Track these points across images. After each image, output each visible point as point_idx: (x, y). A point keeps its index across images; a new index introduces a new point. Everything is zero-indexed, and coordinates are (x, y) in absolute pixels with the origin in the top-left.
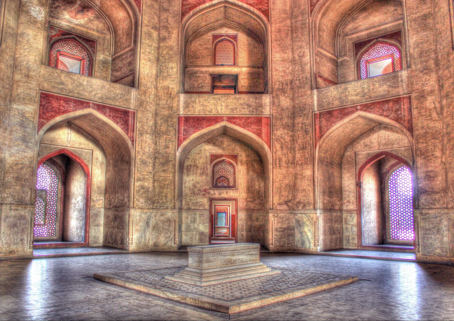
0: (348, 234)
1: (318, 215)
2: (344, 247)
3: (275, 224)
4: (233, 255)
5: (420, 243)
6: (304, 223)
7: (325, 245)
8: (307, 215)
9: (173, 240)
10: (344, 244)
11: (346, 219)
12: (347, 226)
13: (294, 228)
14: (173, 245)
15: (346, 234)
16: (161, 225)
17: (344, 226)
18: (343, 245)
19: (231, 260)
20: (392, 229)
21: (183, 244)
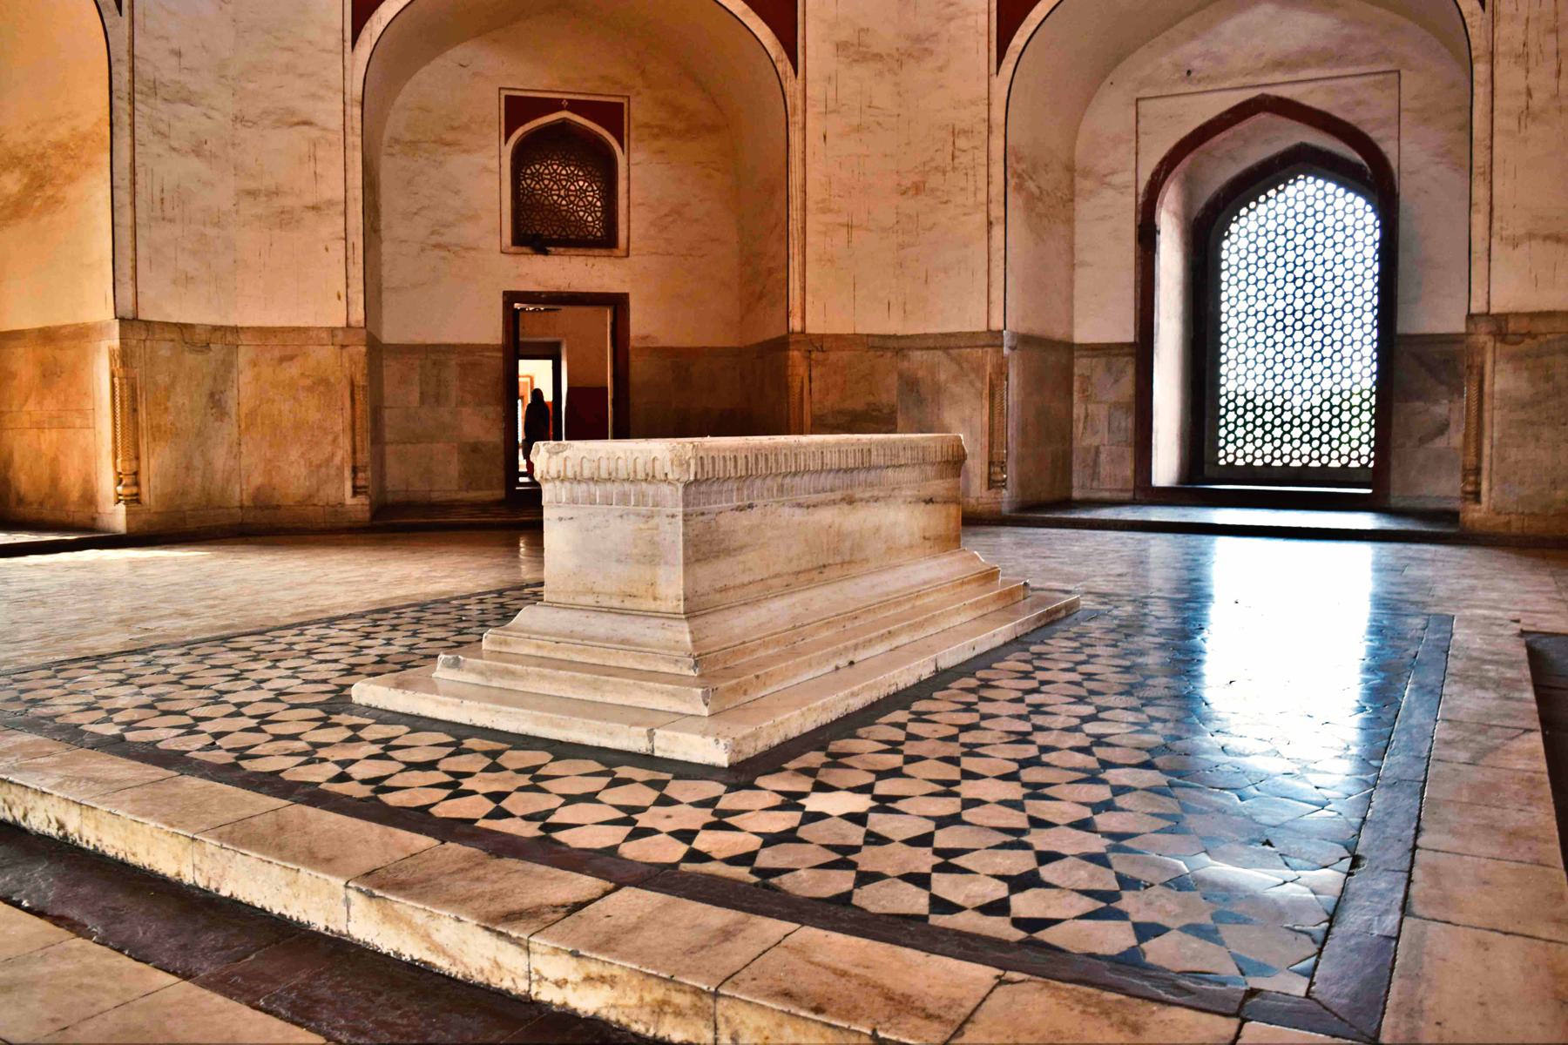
0: (1095, 441)
1: (1006, 351)
2: (1077, 494)
3: (816, 397)
4: (850, 501)
5: (1485, 465)
6: (938, 390)
7: (1023, 485)
8: (954, 352)
9: (348, 473)
10: (1076, 481)
11: (1086, 379)
12: (1091, 407)
13: (893, 412)
14: (349, 500)
15: (1086, 443)
16: (286, 407)
17: (1078, 411)
18: (1070, 487)
19: (841, 536)
20: (1226, 425)
21: (390, 498)
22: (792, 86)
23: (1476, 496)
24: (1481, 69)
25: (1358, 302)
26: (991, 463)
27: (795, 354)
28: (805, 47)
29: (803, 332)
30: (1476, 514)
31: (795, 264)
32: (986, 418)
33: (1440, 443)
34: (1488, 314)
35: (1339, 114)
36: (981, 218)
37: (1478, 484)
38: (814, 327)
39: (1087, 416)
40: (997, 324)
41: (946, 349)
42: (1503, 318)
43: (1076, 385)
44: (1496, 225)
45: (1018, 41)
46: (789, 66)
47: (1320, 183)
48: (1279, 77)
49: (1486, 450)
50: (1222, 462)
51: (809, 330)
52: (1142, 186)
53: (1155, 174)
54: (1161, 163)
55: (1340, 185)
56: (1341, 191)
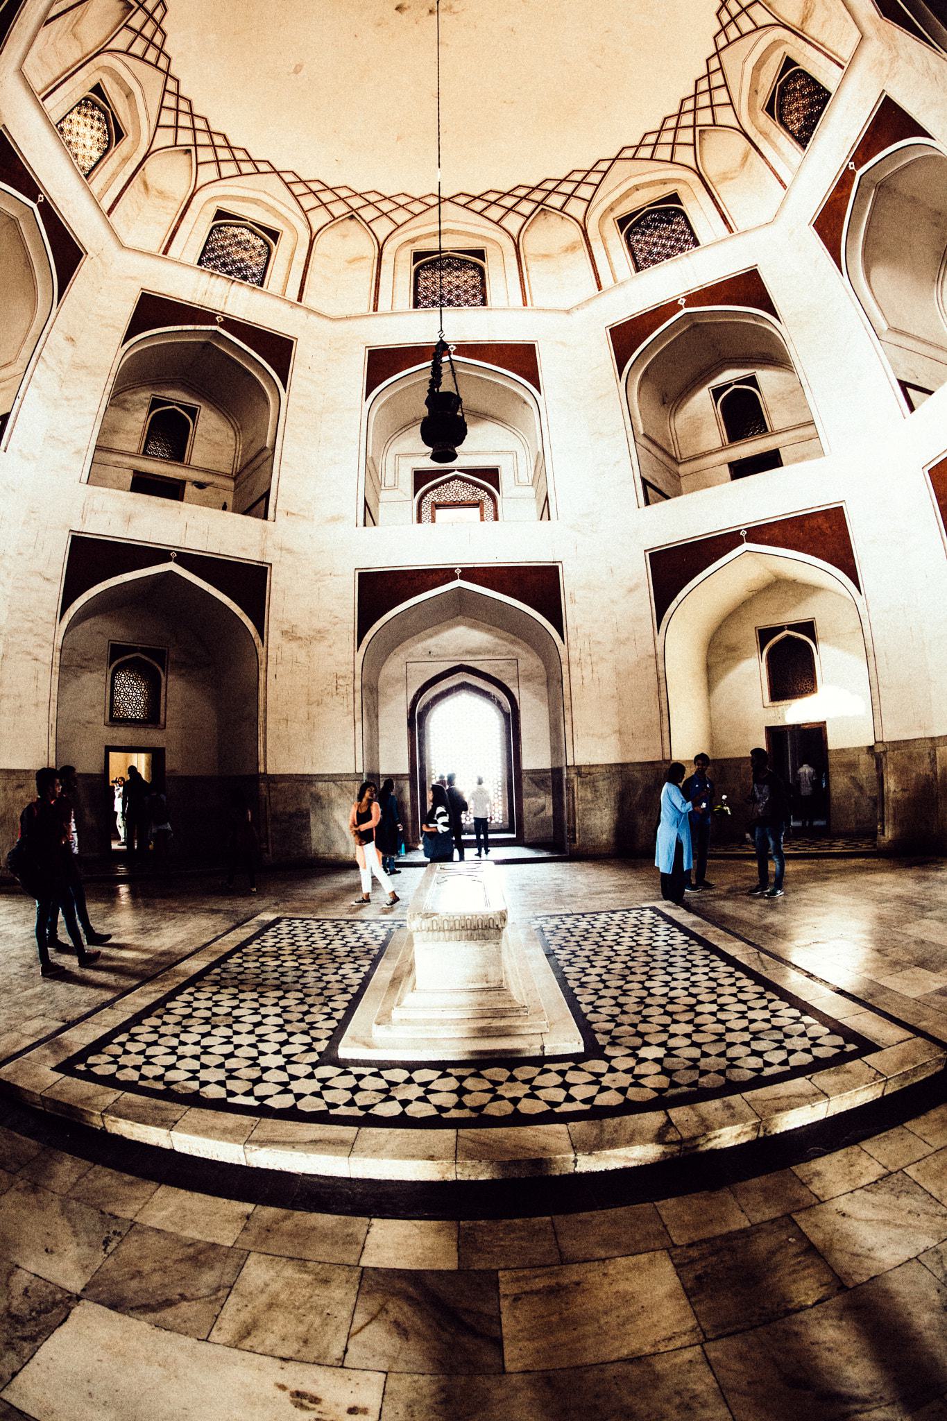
6: (331, 802)
29: (265, 773)
31: (261, 738)
36: (350, 718)
40: (359, 770)
41: (334, 781)
45: (368, 637)
48: (468, 657)
51: (270, 772)
53: (415, 696)
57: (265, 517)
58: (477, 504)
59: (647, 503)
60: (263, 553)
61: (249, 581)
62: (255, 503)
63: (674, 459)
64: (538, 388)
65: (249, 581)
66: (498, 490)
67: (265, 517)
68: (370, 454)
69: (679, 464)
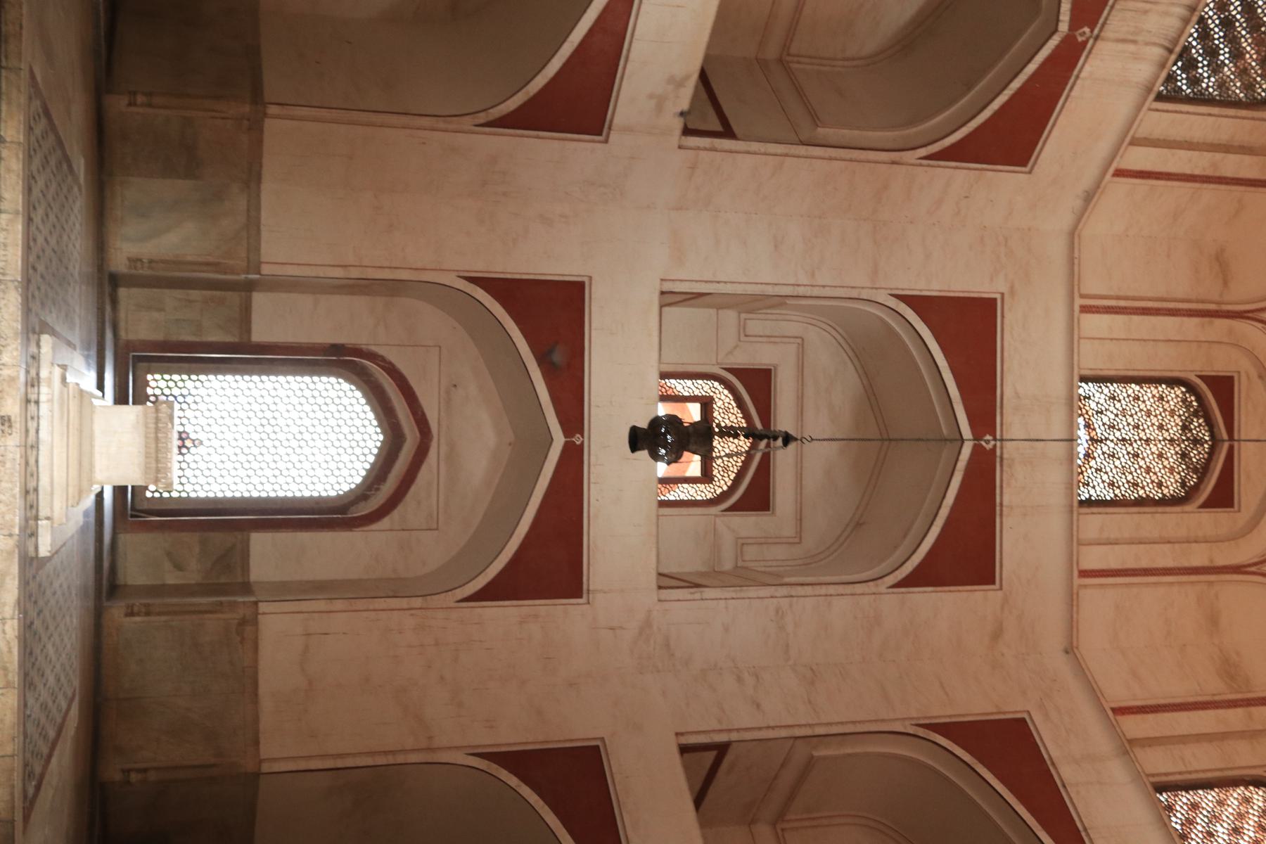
22: (467, 122)
23: (131, 614)
24: (417, 602)
25: (281, 480)
26: (151, 261)
27: (246, 109)
28: (494, 134)
29: (265, 115)
30: (116, 611)
31: (324, 113)
32: (189, 258)
33: (167, 565)
34: (257, 614)
35: (413, 489)
37: (138, 614)
38: (268, 123)
39: (190, 301)
40: (266, 270)
42: (255, 622)
43: (218, 293)
44: (316, 615)
46: (482, 121)
47: (375, 451)
48: (444, 449)
49: (163, 618)
50: (149, 377)
52: (374, 349)
53: (383, 359)
54: (390, 363)
55: (373, 465)
56: (368, 467)
57: (687, 131)
58: (707, 476)
59: (684, 750)
60: (628, 129)
61: (579, 104)
62: (713, 111)
63: (781, 816)
64: (899, 585)
65: (579, 104)
66: (733, 508)
67: (687, 131)
68: (789, 302)
69: (774, 825)
